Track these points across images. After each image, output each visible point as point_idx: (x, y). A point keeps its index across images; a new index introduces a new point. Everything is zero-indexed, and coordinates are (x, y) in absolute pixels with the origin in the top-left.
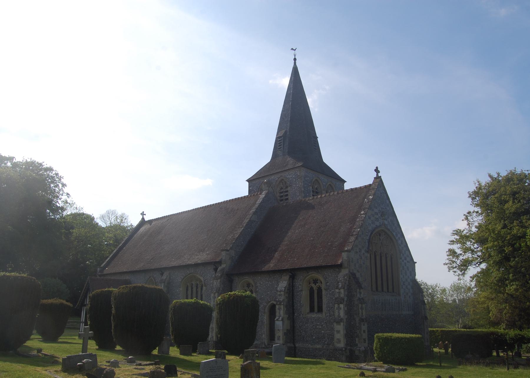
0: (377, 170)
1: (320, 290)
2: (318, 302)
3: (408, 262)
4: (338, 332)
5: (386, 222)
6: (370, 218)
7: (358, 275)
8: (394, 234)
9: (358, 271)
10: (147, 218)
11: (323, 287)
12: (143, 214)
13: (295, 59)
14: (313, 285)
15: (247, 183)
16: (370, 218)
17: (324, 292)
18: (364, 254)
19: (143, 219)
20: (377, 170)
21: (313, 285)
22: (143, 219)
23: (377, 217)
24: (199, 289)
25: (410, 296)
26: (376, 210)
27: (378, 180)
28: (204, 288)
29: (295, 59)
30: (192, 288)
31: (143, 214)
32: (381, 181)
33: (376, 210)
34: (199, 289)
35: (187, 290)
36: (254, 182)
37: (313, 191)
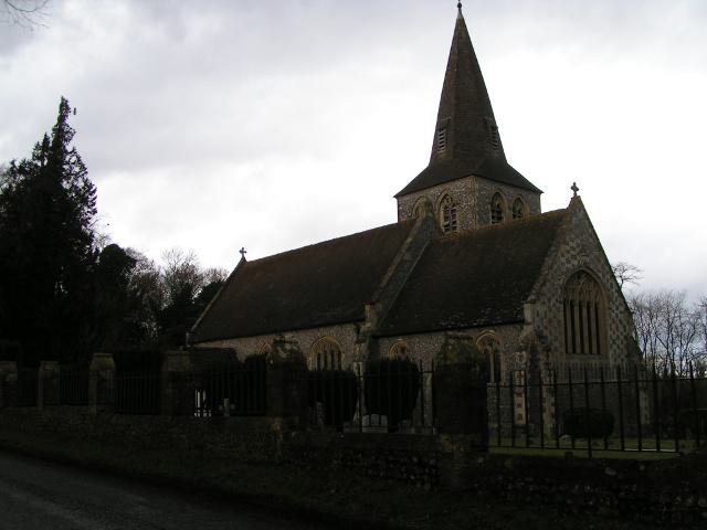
0: (575, 188)
1: (496, 351)
2: (495, 370)
3: (621, 312)
4: (520, 406)
5: (588, 260)
6: (563, 256)
7: (546, 333)
8: (600, 275)
9: (546, 328)
10: (250, 258)
11: (501, 348)
12: (242, 252)
13: (460, 6)
14: (488, 347)
15: (395, 200)
16: (563, 256)
17: (502, 358)
18: (554, 305)
19: (243, 259)
20: (575, 188)
21: (488, 347)
22: (243, 259)
23: (574, 253)
24: (336, 359)
25: (622, 360)
26: (571, 244)
27: (576, 203)
28: (343, 356)
29: (460, 6)
30: (326, 357)
31: (242, 252)
32: (580, 202)
33: (571, 244)
34: (336, 359)
35: (319, 359)
36: (406, 198)
37: (493, 211)
